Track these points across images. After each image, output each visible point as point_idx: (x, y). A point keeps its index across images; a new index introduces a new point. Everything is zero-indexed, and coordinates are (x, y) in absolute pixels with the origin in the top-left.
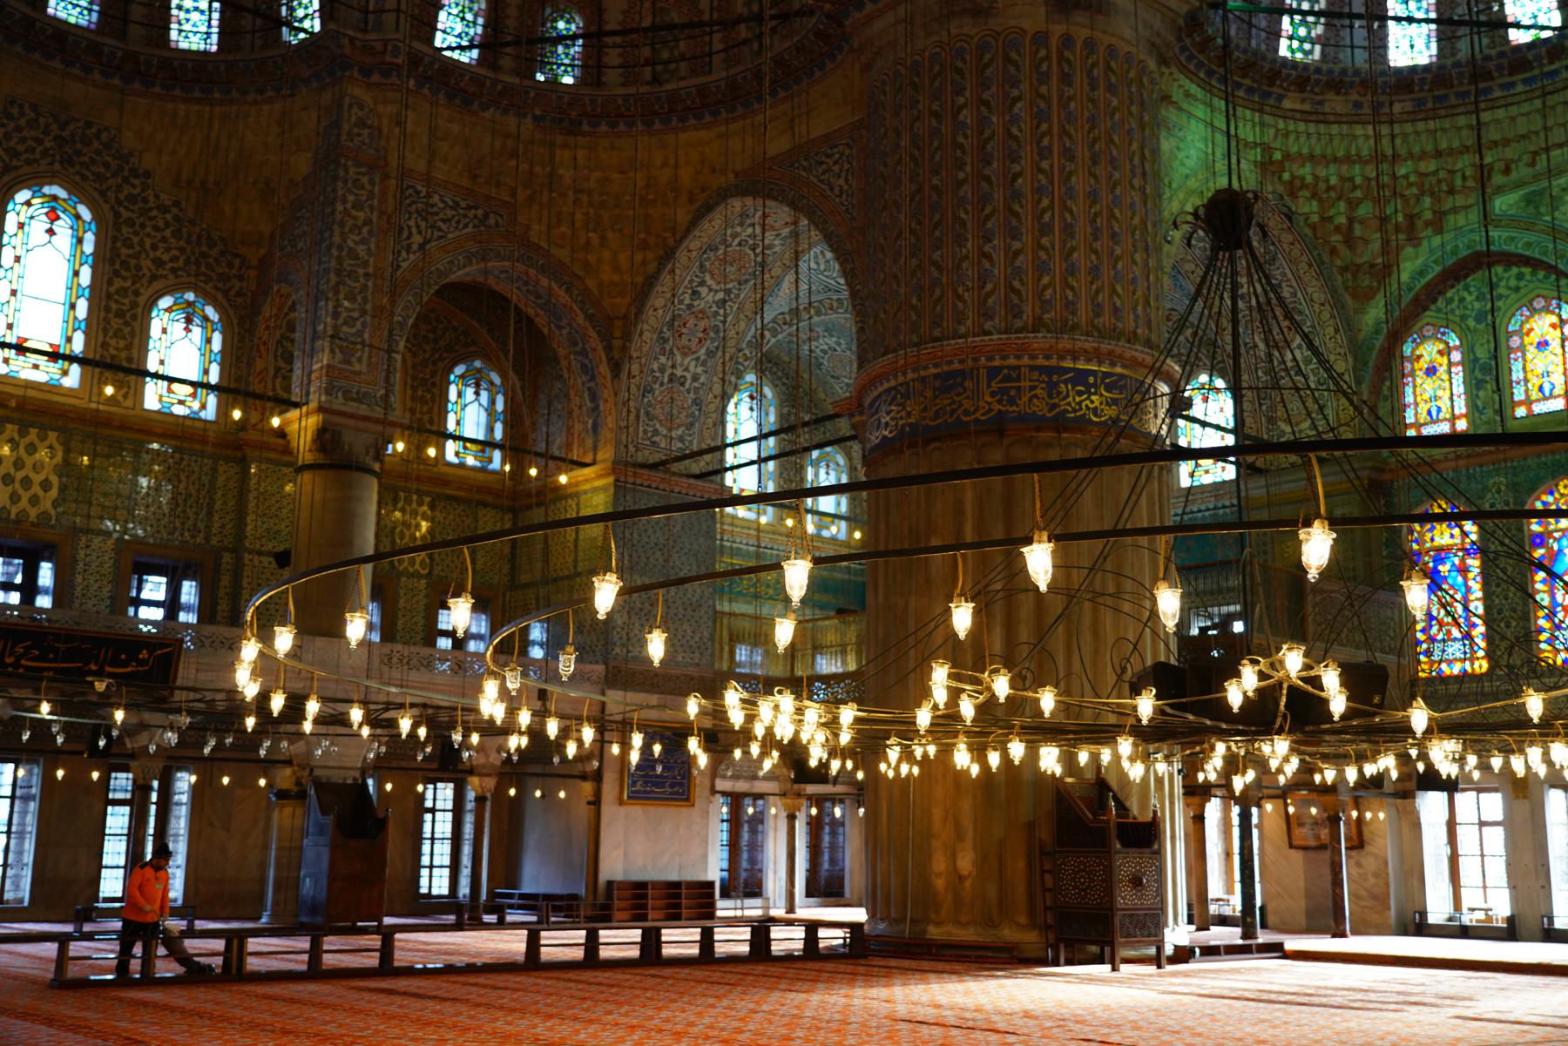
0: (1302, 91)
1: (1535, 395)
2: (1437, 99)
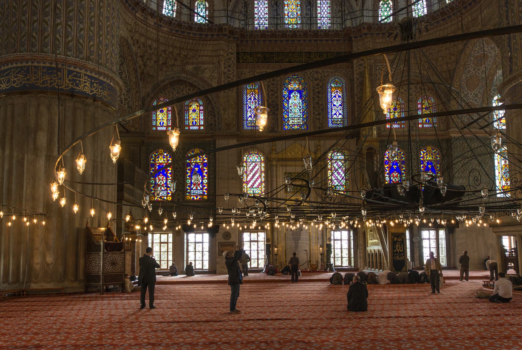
0: (143, 12)
1: (191, 124)
2: (177, 31)
